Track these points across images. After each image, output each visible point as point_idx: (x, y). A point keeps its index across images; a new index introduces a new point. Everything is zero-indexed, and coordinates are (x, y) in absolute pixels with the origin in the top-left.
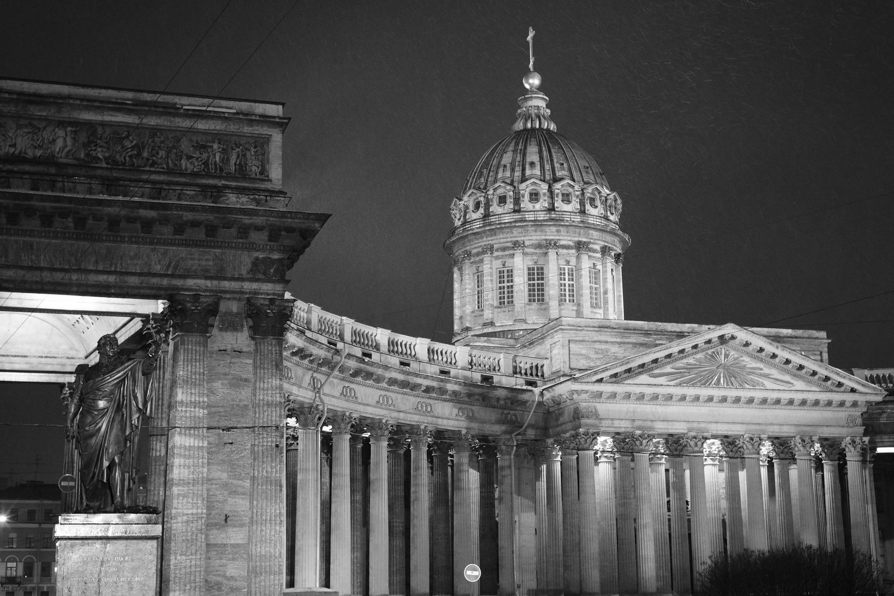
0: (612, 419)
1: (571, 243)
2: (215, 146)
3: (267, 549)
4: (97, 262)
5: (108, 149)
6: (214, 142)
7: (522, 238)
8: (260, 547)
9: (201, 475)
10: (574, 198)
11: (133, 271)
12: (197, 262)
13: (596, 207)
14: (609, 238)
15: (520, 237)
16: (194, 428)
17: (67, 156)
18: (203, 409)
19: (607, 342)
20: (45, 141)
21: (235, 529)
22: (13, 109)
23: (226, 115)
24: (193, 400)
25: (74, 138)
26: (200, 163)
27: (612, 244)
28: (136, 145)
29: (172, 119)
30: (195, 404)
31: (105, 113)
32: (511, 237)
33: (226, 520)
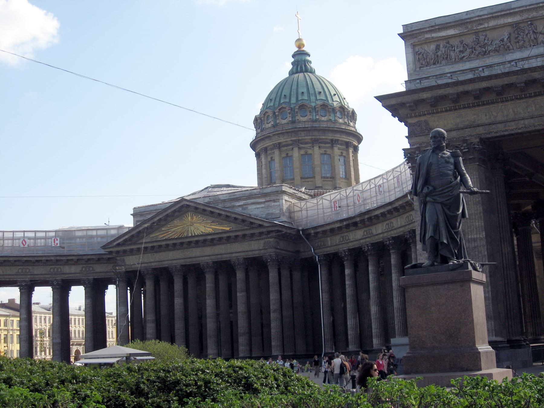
7: (264, 146)
14: (316, 133)
27: (320, 136)
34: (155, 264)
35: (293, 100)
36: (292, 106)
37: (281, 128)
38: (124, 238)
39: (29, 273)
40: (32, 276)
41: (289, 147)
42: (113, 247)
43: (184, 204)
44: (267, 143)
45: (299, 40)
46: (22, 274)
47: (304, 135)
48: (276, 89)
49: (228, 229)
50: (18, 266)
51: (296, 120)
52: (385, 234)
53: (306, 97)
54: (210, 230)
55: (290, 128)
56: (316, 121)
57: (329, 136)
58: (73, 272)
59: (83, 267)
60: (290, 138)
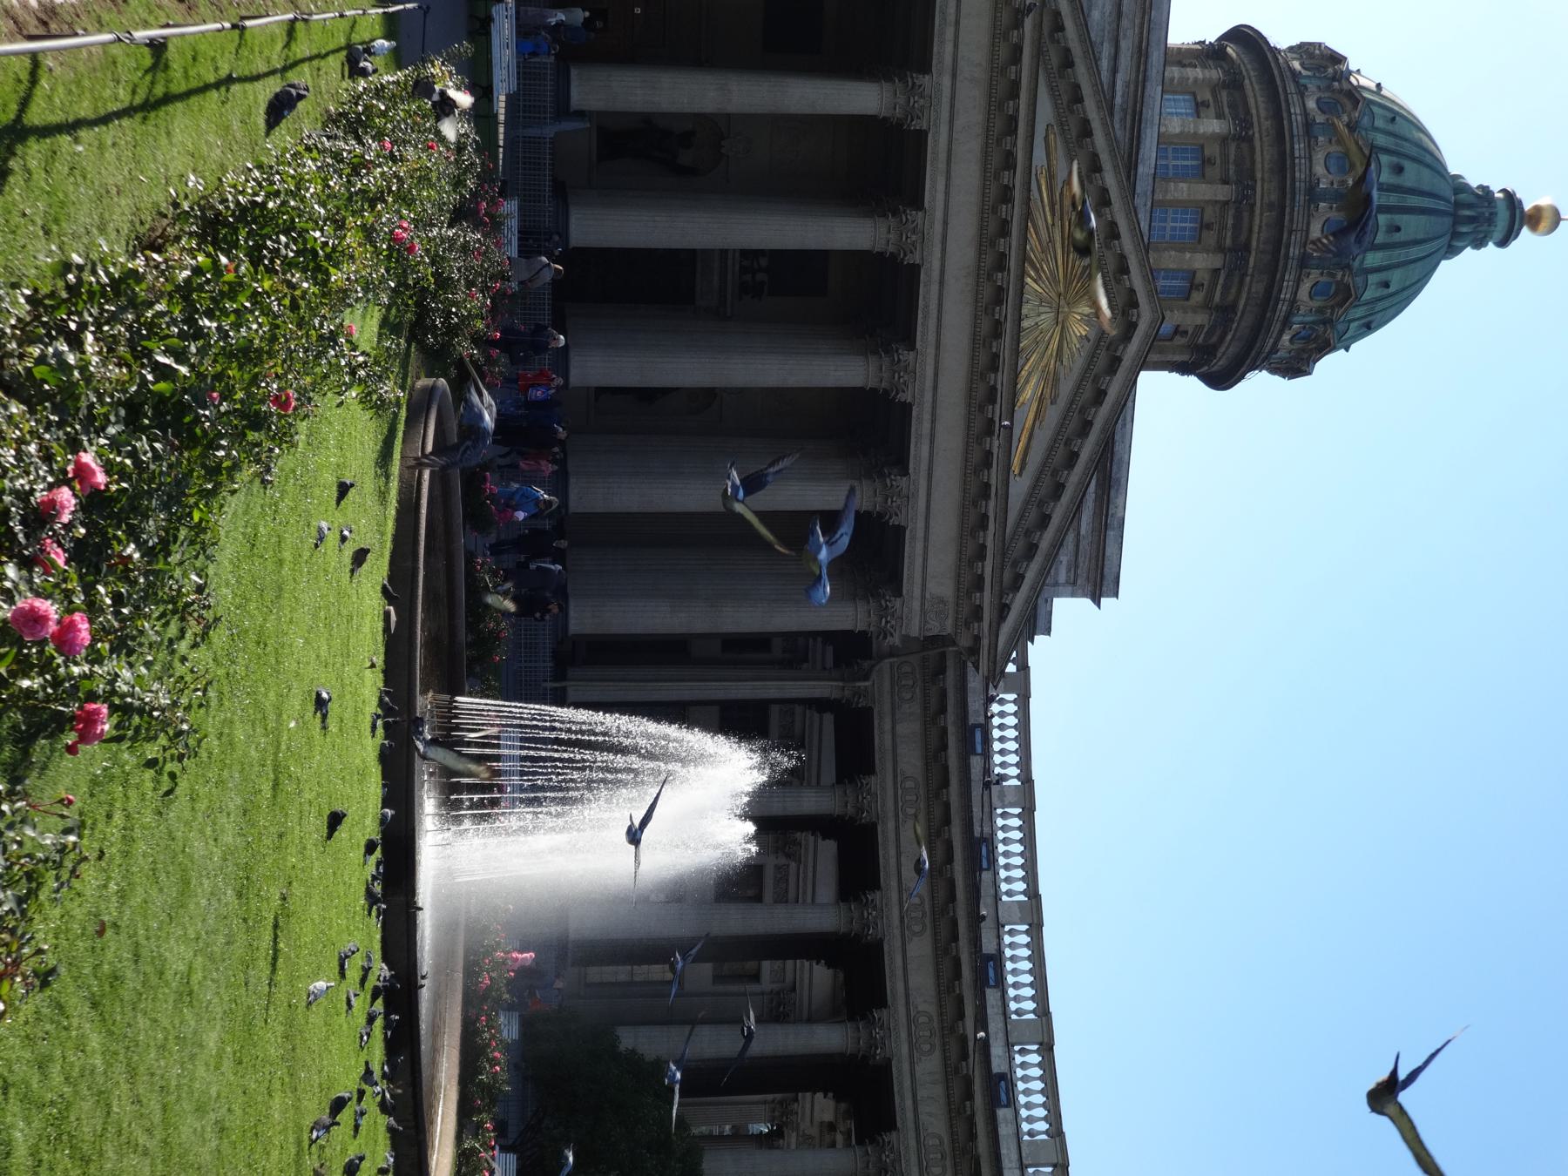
0: (957, 23)
1: (1243, 238)
7: (1257, 135)
15: (1260, 132)
19: (1114, 71)
32: (1258, 116)
35: (1373, 259)
36: (1356, 264)
37: (1300, 225)
38: (1069, 23)
41: (1229, 234)
43: (1138, 315)
44: (1264, 155)
45: (1557, 219)
47: (1253, 290)
48: (1426, 180)
51: (1308, 271)
52: (902, 1010)
55: (1292, 250)
56: (1286, 323)
57: (1227, 348)
60: (1258, 246)
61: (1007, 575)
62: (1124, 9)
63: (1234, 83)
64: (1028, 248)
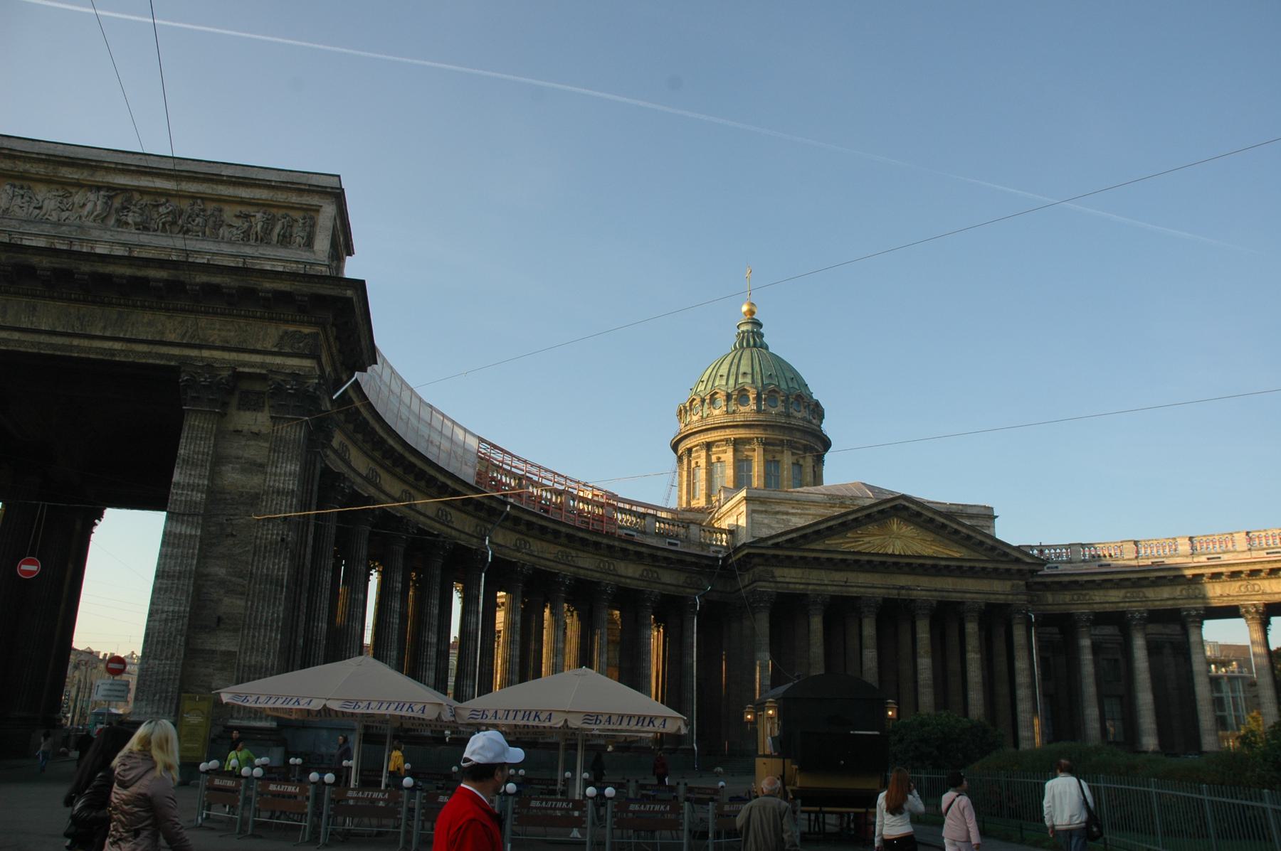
1: (777, 442)
2: (259, 215)
3: (259, 659)
4: (105, 328)
5: (141, 215)
6: (258, 212)
7: (734, 436)
8: (250, 655)
9: (188, 568)
10: (780, 403)
11: (145, 338)
12: (216, 332)
13: (799, 412)
16: (189, 515)
17: (95, 221)
18: (202, 492)
19: (787, 514)
20: (76, 206)
21: (227, 634)
22: (43, 170)
23: (273, 184)
24: (191, 482)
25: (106, 203)
26: (239, 232)
28: (171, 211)
29: (215, 186)
30: (192, 487)
31: (142, 178)
33: (218, 625)
34: (834, 588)
35: (783, 386)
39: (572, 563)
40: (575, 569)
42: (768, 548)
43: (901, 504)
45: (752, 304)
46: (563, 562)
49: (957, 555)
50: (560, 545)
53: (797, 387)
54: (928, 550)
56: (810, 422)
58: (630, 575)
59: (646, 570)
61: (1003, 559)
62: (764, 509)
63: (709, 446)
64: (872, 552)
